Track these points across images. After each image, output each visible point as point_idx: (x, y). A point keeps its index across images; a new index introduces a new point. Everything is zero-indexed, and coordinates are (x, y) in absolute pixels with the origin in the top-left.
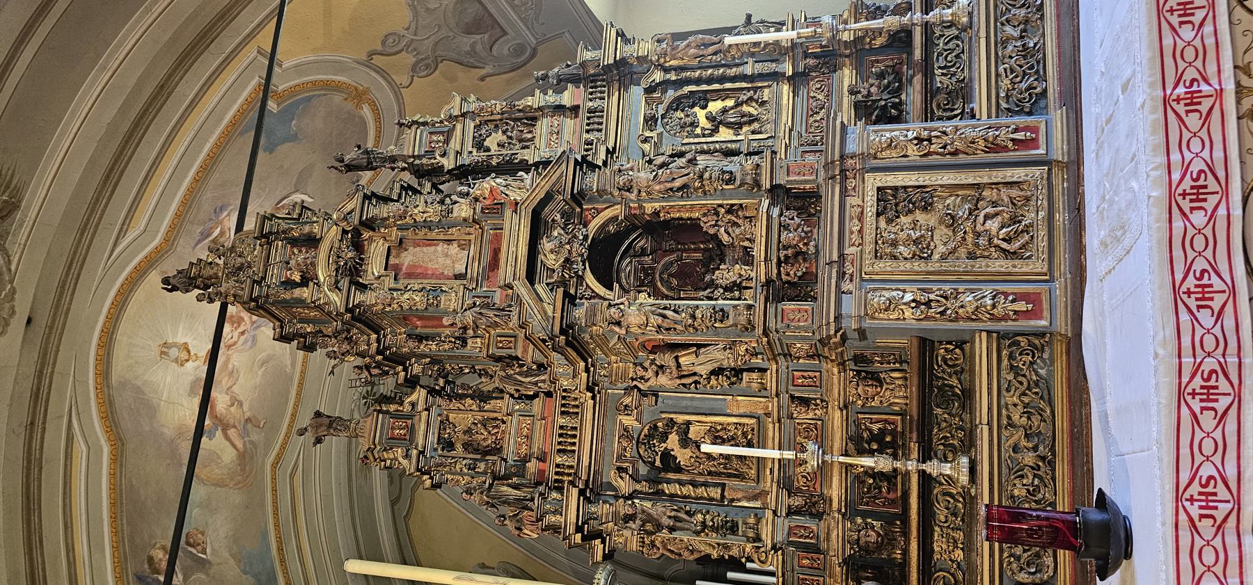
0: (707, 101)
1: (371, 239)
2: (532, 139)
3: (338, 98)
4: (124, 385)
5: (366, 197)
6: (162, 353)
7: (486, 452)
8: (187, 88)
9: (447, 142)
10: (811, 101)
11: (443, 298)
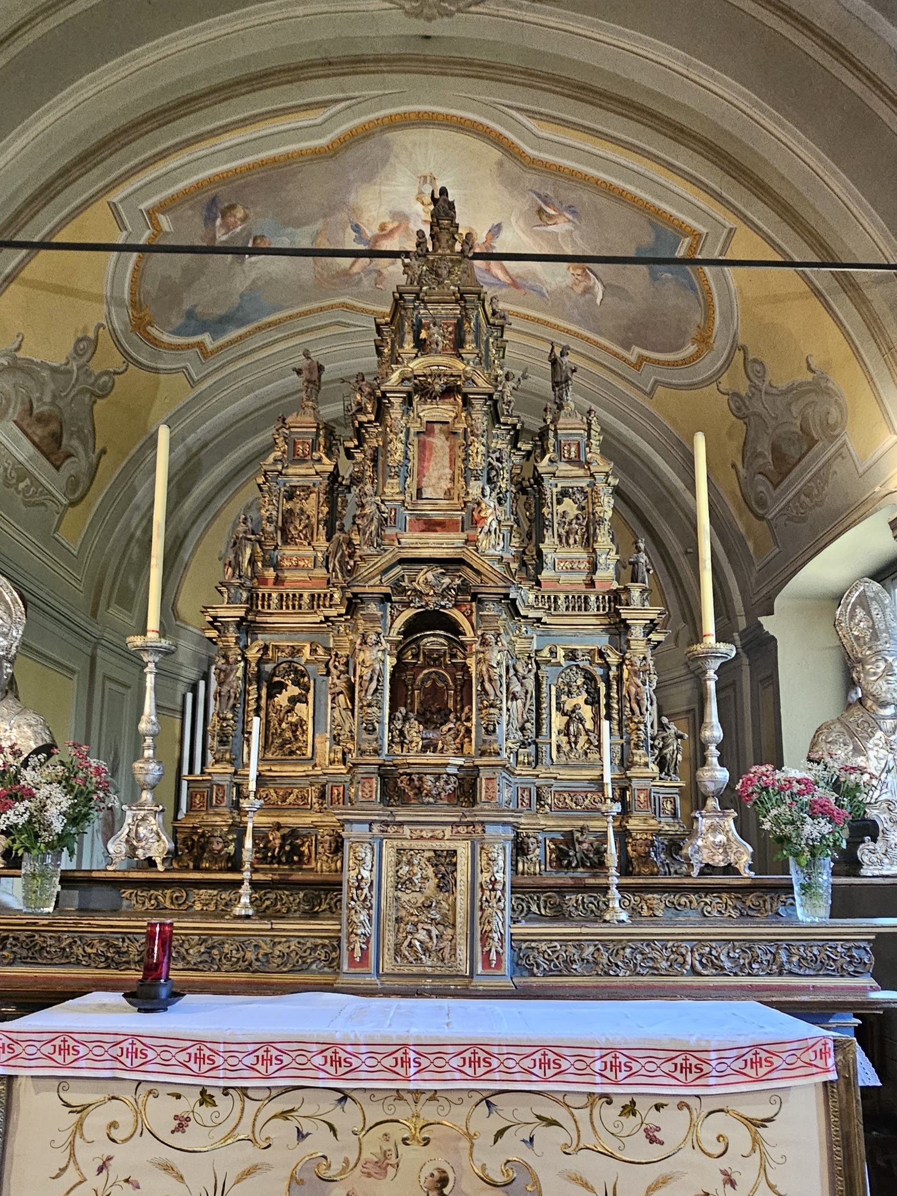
0: (592, 704)
1: (455, 404)
2: (568, 544)
3: (698, 318)
4: (387, 145)
5: (490, 396)
6: (425, 177)
7: (284, 531)
8: (684, 159)
9: (570, 461)
10: (583, 795)
11: (395, 481)
